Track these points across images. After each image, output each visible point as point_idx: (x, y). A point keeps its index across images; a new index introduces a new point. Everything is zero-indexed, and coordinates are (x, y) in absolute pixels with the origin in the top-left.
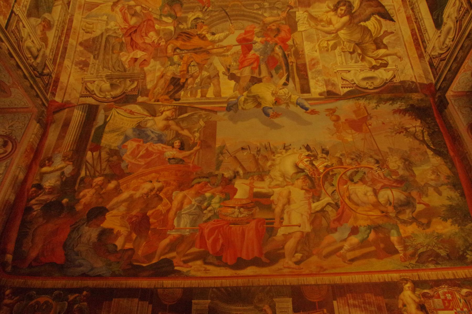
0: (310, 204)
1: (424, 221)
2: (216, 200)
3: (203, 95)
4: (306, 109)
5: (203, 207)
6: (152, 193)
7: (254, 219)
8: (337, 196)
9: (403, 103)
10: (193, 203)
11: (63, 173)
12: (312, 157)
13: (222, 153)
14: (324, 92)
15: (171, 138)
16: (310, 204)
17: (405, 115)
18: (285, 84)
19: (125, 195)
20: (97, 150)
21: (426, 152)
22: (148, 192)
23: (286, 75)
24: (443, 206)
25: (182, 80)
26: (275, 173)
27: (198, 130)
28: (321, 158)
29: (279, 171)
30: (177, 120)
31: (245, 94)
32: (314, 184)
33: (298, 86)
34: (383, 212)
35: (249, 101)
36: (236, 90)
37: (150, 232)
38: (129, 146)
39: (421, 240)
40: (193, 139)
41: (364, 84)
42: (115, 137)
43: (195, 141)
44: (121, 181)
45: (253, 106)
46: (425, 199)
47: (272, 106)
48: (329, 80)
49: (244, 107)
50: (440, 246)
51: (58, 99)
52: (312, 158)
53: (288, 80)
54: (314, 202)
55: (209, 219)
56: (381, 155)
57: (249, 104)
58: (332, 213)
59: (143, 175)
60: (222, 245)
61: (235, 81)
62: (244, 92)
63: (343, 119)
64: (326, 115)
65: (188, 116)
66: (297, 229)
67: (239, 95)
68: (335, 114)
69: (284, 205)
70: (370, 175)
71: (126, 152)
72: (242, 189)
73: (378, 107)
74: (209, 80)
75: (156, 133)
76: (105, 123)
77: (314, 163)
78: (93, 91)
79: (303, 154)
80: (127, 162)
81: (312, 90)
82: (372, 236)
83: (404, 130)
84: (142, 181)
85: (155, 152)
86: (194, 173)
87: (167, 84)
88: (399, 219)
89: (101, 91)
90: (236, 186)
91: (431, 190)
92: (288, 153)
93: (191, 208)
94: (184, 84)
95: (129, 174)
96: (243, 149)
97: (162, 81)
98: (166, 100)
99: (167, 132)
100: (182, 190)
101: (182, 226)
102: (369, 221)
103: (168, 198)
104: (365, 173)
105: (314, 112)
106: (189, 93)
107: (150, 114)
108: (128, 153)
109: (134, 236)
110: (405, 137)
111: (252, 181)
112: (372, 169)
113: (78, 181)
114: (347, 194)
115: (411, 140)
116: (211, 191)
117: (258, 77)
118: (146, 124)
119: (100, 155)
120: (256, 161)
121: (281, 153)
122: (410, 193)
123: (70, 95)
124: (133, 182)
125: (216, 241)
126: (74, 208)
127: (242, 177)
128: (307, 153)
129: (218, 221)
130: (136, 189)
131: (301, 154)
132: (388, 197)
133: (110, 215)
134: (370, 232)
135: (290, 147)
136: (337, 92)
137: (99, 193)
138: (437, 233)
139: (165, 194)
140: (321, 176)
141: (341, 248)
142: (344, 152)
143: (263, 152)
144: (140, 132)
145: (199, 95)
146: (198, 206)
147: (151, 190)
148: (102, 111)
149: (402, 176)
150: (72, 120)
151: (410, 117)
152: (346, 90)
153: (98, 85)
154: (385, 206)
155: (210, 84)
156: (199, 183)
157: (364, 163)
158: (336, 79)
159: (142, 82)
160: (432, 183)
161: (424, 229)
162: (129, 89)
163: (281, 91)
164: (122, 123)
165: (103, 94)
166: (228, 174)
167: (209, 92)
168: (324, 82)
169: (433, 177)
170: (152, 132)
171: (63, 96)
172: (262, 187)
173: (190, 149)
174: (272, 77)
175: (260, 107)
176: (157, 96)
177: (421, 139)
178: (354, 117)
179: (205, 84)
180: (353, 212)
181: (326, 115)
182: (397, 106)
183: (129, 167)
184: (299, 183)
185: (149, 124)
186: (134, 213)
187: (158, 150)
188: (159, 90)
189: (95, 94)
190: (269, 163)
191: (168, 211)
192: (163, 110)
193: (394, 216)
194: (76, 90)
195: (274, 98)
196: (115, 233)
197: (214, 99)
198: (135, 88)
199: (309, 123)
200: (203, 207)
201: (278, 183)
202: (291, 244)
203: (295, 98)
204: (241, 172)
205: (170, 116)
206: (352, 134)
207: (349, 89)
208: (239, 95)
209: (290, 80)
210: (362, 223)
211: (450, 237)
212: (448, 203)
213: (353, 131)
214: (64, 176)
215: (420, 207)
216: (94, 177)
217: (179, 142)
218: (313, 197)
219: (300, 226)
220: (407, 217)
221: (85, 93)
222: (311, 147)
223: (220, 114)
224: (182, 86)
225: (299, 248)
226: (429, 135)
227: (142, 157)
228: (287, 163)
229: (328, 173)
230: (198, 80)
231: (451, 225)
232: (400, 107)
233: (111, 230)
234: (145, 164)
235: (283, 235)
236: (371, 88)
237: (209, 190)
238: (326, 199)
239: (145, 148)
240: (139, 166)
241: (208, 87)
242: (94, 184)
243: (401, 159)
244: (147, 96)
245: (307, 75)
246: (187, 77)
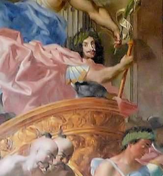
6: (55, 162)
15: (76, 32)
22: (46, 158)
43: (124, 42)
59: (33, 119)
86: (126, 120)
100: (106, 157)
116: (158, 159)
124: (16, 134)
130: (24, 151)
139: (78, 163)
147: (53, 155)
156: (136, 141)
170: (37, 13)
173: (116, 60)
187: (55, 62)
227: (25, 77)
234: (33, 95)
237: (153, 159)
239: (27, 57)
240: (23, 99)
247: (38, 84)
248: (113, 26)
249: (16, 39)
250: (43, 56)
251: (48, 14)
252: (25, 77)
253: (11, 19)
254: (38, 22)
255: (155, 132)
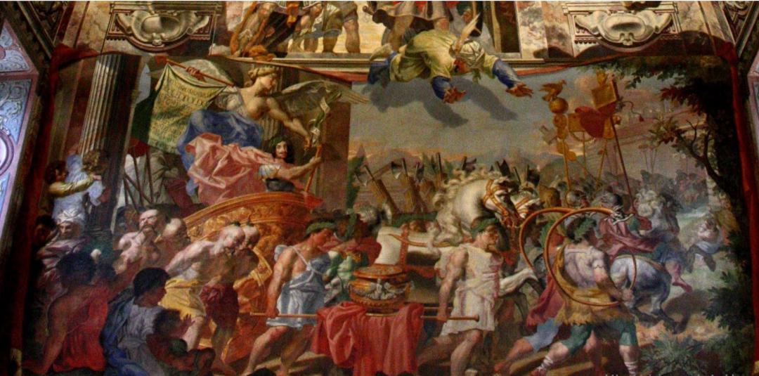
0: (497, 280)
1: (677, 318)
2: (345, 265)
3: (328, 48)
4: (510, 84)
5: (324, 278)
6: (241, 247)
7: (406, 303)
8: (543, 266)
9: (683, 76)
10: (308, 269)
11: (87, 197)
12: (510, 188)
13: (358, 173)
14: (543, 50)
15: (270, 137)
16: (497, 280)
17: (682, 103)
18: (475, 34)
19: (195, 248)
20: (142, 155)
21: (704, 182)
22: (233, 244)
23: (477, 17)
24: (714, 289)
25: (291, 19)
26: (446, 217)
27: (318, 121)
28: (525, 189)
29: (453, 213)
30: (280, 98)
31: (402, 49)
32: (507, 236)
33: (498, 38)
34: (613, 299)
35: (410, 64)
36: (387, 42)
37: (238, 320)
38: (198, 150)
39: (667, 352)
40: (308, 139)
41: (616, 36)
42: (173, 128)
43: (313, 146)
44: (187, 220)
45: (416, 75)
46: (686, 277)
47: (449, 76)
48: (553, 28)
49: (400, 76)
50: (694, 364)
51: (67, 42)
52: (510, 190)
53: (479, 25)
54: (504, 277)
55: (334, 300)
56: (626, 187)
57: (409, 69)
58: (531, 298)
60: (354, 349)
61: (385, 24)
62: (401, 45)
63: (571, 108)
64: (544, 98)
65: (302, 88)
66: (472, 324)
67: (392, 52)
68: (559, 96)
69: (456, 280)
70: (602, 228)
71: (193, 162)
72: (389, 245)
73: (637, 83)
74: (338, 21)
75: (244, 124)
76: (154, 94)
77: (512, 199)
78: (130, 29)
79: (496, 181)
80: (196, 181)
81: (523, 46)
82: (591, 342)
83: (672, 135)
84: (223, 222)
85: (242, 162)
86: (311, 211)
87: (263, 25)
88: (638, 313)
89: (144, 29)
90: (379, 240)
91: (699, 260)
92: (470, 178)
93: (304, 278)
94: (294, 25)
95: (200, 206)
96: (394, 165)
97: (255, 19)
98: (261, 53)
99: (263, 122)
100: (290, 244)
101: (289, 312)
102: (590, 315)
103: (266, 258)
104: (595, 223)
105: (523, 91)
106: (303, 42)
107: (233, 81)
108: (197, 163)
109: (213, 325)
110: (675, 149)
111: (406, 231)
112: (608, 214)
113: (115, 214)
114: (560, 263)
115: (684, 156)
116: (339, 247)
117: (427, 18)
118: (226, 103)
119: (148, 164)
120: (415, 191)
121: (458, 177)
122: (663, 265)
123: (88, 33)
124: (207, 222)
125: (343, 341)
126: (113, 269)
127: (390, 222)
128: (502, 179)
129: (348, 305)
130: (214, 237)
131: (492, 181)
132: (627, 271)
133: (174, 284)
134: (588, 337)
135: (475, 165)
136: (568, 51)
137: (152, 243)
138: (695, 341)
139: (262, 249)
140: (522, 226)
141: (540, 362)
142: (565, 179)
143: (428, 175)
144: (217, 118)
145: (320, 49)
146: (315, 275)
147: (240, 240)
148: (146, 69)
149: (656, 231)
150: (93, 87)
151: (691, 106)
152: (583, 47)
153: (138, 19)
154: (619, 288)
155: (341, 29)
156: (318, 231)
157: (597, 204)
158: (565, 26)
159: (219, 18)
160: (704, 246)
161: (675, 333)
162: (195, 30)
163: (467, 46)
164: (182, 97)
165: (148, 36)
166: (366, 216)
167: (338, 42)
168: (543, 32)
169: (707, 234)
170: (238, 121)
171: (75, 35)
172: (422, 243)
173: (305, 160)
174: (451, 19)
175: (429, 76)
176: (245, 44)
177: (701, 154)
178: (591, 103)
179: (332, 27)
180: (567, 298)
181: (544, 98)
182: (669, 82)
183: (200, 191)
184: (483, 237)
185: (232, 103)
186: (212, 283)
187: (249, 160)
188: (248, 34)
189: (133, 35)
190: (436, 198)
191: (268, 282)
192: (255, 74)
193: (631, 307)
194: (99, 25)
195: (453, 60)
196: (182, 318)
197: (347, 56)
198: (205, 28)
199: (512, 116)
200: (324, 278)
201: (449, 236)
202: (461, 351)
203: (490, 59)
204: (389, 213)
205: (268, 87)
206: (583, 141)
207: (588, 45)
208: (392, 52)
209: (485, 26)
210: (579, 318)
211: (713, 349)
212: (721, 284)
213: (587, 136)
214: (90, 203)
215: (675, 292)
216: (142, 209)
217: (284, 146)
218: (504, 267)
219: (477, 320)
220: (651, 310)
221: (115, 32)
222: (511, 166)
223: (357, 88)
224: (291, 30)
225: (474, 359)
226: (716, 146)
227: (221, 173)
228: (467, 198)
229: (532, 221)
230: (319, 20)
231: (719, 326)
232: (676, 83)
233: (177, 312)
234: (228, 188)
235: (451, 335)
236: (628, 44)
237: (334, 246)
238: (526, 272)
239: (226, 156)
240: (217, 191)
241: (337, 34)
242: (142, 224)
243: (658, 197)
244: (227, 43)
245: (514, 18)
246: (301, 13)
247: (233, 179)
248: (304, 132)
249: (216, 140)
250: (239, 156)
251: (248, 122)
252: (221, 173)
253: (215, 125)
254: (238, 128)
255: (338, 222)
